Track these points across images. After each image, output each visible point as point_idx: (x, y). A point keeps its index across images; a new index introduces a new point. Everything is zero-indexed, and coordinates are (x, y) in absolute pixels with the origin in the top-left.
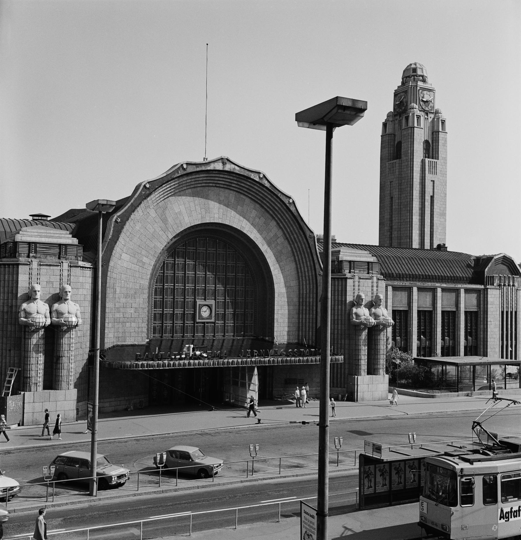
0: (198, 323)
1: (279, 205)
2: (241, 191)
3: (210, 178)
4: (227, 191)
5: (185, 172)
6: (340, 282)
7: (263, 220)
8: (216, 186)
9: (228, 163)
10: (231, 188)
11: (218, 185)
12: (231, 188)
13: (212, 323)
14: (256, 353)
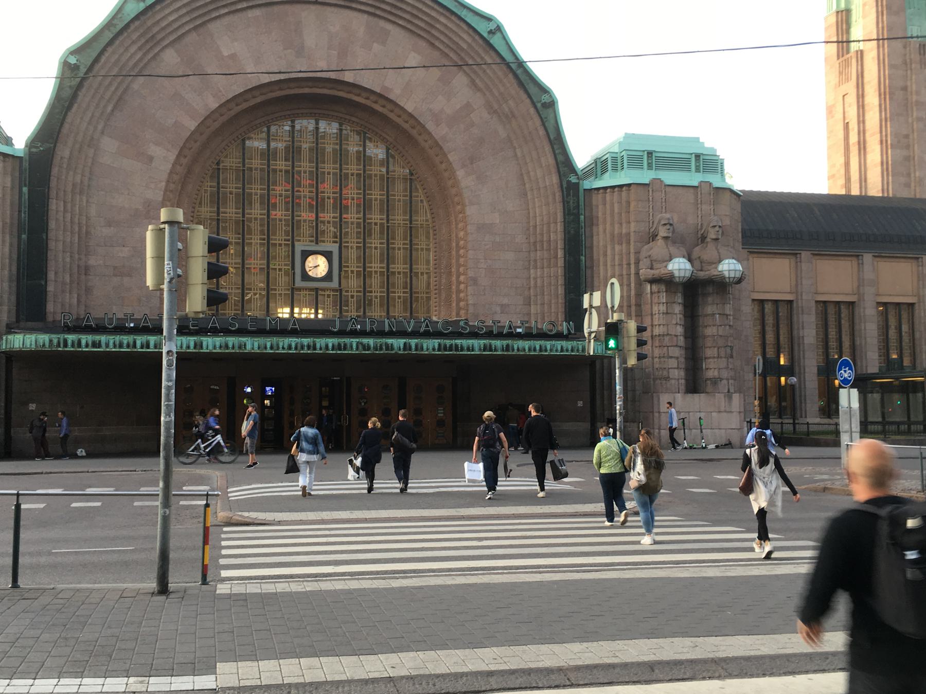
0: (299, 289)
1: (465, 36)
2: (378, 12)
7: (436, 72)
13: (334, 290)
14: (300, 313)
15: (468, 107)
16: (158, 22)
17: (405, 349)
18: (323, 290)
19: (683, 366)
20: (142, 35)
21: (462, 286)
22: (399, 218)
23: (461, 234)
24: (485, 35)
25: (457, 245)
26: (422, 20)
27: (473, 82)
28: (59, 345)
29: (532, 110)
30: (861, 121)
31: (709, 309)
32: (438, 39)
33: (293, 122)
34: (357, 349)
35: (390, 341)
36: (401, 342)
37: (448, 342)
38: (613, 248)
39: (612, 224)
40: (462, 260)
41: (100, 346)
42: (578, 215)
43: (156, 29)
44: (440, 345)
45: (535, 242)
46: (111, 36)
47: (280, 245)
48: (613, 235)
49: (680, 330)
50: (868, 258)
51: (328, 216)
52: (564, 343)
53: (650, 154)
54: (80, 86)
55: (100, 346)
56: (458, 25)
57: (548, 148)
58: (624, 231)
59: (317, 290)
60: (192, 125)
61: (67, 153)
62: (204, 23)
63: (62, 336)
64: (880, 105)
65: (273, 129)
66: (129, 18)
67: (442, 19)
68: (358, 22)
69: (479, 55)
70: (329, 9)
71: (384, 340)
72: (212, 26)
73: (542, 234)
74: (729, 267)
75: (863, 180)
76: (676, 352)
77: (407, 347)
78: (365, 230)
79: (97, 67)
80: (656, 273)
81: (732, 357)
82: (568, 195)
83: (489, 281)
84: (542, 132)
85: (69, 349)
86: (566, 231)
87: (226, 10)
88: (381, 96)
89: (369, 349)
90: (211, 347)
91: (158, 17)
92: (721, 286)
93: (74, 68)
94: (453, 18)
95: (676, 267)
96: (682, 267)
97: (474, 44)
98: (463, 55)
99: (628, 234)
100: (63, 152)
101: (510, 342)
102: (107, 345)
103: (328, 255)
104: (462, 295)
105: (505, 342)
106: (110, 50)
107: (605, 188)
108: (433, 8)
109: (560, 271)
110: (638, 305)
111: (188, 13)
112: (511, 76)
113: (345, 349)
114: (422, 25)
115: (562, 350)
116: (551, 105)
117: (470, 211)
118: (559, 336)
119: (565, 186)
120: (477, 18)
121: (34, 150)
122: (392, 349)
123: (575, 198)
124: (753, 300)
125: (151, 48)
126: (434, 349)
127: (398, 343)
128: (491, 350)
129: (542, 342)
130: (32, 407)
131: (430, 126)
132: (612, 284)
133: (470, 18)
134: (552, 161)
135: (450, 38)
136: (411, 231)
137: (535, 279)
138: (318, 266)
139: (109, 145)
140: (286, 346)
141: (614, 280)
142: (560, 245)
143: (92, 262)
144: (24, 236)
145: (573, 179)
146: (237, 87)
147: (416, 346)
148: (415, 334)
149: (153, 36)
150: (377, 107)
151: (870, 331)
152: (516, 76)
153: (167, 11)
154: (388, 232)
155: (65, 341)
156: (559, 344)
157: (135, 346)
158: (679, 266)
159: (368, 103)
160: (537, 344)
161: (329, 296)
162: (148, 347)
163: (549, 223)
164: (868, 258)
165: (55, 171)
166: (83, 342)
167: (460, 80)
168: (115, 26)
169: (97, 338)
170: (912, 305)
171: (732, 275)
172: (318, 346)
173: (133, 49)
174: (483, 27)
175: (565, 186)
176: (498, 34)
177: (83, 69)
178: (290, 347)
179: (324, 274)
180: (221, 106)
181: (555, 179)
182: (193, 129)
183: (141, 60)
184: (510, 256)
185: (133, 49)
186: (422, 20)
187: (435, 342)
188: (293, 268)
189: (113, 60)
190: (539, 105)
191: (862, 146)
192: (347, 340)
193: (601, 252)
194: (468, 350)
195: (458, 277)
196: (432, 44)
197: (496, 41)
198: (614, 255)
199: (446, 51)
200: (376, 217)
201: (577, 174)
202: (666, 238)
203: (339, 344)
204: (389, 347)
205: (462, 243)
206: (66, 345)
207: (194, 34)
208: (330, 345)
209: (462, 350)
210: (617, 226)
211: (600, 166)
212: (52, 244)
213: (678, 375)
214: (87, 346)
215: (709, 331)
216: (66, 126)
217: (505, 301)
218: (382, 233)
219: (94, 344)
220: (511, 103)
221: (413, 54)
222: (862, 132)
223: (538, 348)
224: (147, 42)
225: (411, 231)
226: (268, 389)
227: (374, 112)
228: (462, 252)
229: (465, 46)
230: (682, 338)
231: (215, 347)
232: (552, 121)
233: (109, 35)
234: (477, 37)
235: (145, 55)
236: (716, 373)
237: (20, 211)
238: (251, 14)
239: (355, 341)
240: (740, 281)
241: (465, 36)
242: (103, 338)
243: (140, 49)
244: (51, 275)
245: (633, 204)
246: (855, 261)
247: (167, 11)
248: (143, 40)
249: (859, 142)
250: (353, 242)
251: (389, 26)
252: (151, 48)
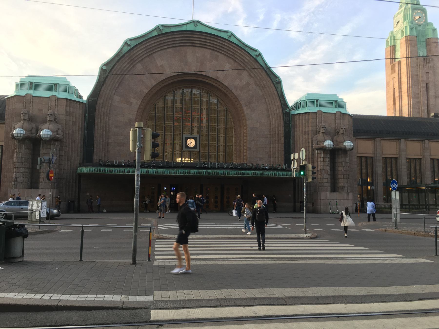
0: (185, 151)
1: (247, 57)
2: (215, 49)
3: (185, 38)
4: (203, 49)
5: (160, 33)
6: (301, 117)
8: (192, 46)
9: (199, 24)
10: (206, 47)
11: (194, 45)
12: (206, 47)
13: (197, 152)
14: (185, 160)
16: (135, 54)
17: (223, 174)
18: (194, 152)
19: (330, 182)
20: (129, 58)
21: (245, 151)
22: (222, 125)
23: (245, 131)
24: (255, 57)
25: (243, 135)
26: (231, 51)
27: (250, 74)
28: (98, 171)
29: (272, 85)
30: (400, 88)
31: (340, 160)
32: (237, 58)
33: (183, 90)
34: (206, 174)
35: (218, 171)
36: (222, 171)
37: (240, 172)
38: (303, 137)
39: (302, 127)
40: (245, 141)
41: (112, 172)
42: (289, 124)
43: (134, 57)
44: (236, 173)
45: (273, 134)
46: (118, 59)
47: (178, 135)
48: (302, 132)
49: (328, 168)
50: (403, 141)
51: (196, 124)
52: (284, 172)
53: (317, 101)
54: (107, 77)
55: (112, 172)
56: (244, 53)
57: (278, 99)
58: (307, 130)
59: (191, 152)
60: (146, 91)
61: (102, 101)
62: (151, 54)
63: (99, 168)
64: (407, 82)
65: (176, 92)
66: (125, 52)
67: (239, 51)
68: (208, 53)
69: (252, 64)
70: (197, 48)
71: (215, 171)
72: (154, 55)
73: (275, 131)
74: (348, 144)
75: (401, 110)
76: (327, 176)
77: (224, 173)
78: (209, 130)
79: (113, 70)
80: (319, 146)
81: (349, 178)
82: (286, 116)
83: (256, 149)
84: (276, 93)
85: (101, 173)
86: (285, 130)
87: (159, 49)
88: (215, 80)
89: (210, 174)
90: (152, 173)
91: (135, 52)
92: (345, 151)
93: (105, 70)
94: (243, 51)
95: (327, 144)
96: (329, 144)
97: (250, 60)
98: (246, 64)
99: (309, 131)
100: (100, 101)
101: (263, 172)
102: (115, 172)
103: (195, 139)
104: (245, 154)
105: (261, 172)
106: (118, 64)
107: (300, 114)
108: (235, 47)
109: (282, 145)
110: (312, 158)
111: (146, 50)
112: (264, 72)
113: (201, 174)
114: (231, 53)
115: (283, 175)
116: (279, 83)
117: (249, 122)
118: (282, 170)
119: (284, 113)
120: (251, 50)
121: (90, 100)
122: (219, 174)
123: (288, 118)
124: (357, 157)
125: (132, 63)
126: (234, 174)
127: (221, 172)
128: (256, 175)
129: (275, 172)
130: (88, 194)
131: (234, 91)
132: (303, 150)
133: (249, 51)
134: (279, 103)
135: (241, 58)
136: (226, 130)
137: (273, 148)
138: (191, 143)
139: (117, 98)
140: (179, 172)
141: (303, 149)
142: (282, 135)
143: (110, 141)
144: (86, 132)
145: (288, 110)
146: (163, 77)
147: (228, 173)
148: (227, 168)
149: (133, 59)
150: (214, 84)
151: (404, 168)
152: (266, 72)
153: (138, 50)
154: (217, 130)
155: (100, 170)
156: (282, 173)
157: (125, 172)
158: (328, 143)
159: (211, 82)
160: (273, 173)
161: (195, 154)
162: (129, 172)
163: (278, 127)
164: (403, 141)
165: (97, 108)
166: (106, 170)
167: (245, 74)
168: (119, 55)
169: (111, 169)
170: (421, 159)
171: (349, 147)
172: (191, 173)
173: (126, 64)
174: (254, 54)
175: (284, 113)
176: (260, 57)
177: (108, 71)
178: (181, 173)
179: (194, 146)
180: (157, 84)
181: (281, 110)
182: (147, 92)
183: (129, 67)
185: (126, 64)
186: (231, 51)
187: (235, 172)
188: (182, 144)
189: (118, 68)
190: (275, 83)
191: (400, 98)
192: (202, 171)
193: (298, 138)
194: (247, 174)
195: (243, 147)
196: (235, 61)
197: (259, 59)
198: (303, 139)
199: (240, 63)
200: (213, 125)
201: (289, 109)
202: (323, 133)
203: (199, 172)
204: (218, 173)
205: (245, 134)
206: (100, 171)
207: (148, 58)
208: (196, 173)
209: (245, 174)
210: (304, 128)
211: (298, 105)
212: (96, 135)
213: (328, 185)
214: (108, 172)
215: (340, 168)
216: (102, 92)
217: (261, 156)
218: (215, 130)
219: (110, 171)
220: (264, 82)
221: (228, 64)
222: (400, 92)
223: (274, 174)
224: (131, 61)
225: (226, 130)
226: (172, 188)
227: (213, 85)
228: (245, 138)
229: (247, 61)
230: (329, 171)
231: (153, 173)
232: (280, 89)
233: (117, 59)
234: (251, 58)
235: (130, 65)
236: (343, 185)
237: (85, 122)
238: (168, 50)
239: (205, 171)
240: (352, 149)
241: (247, 57)
242: (113, 169)
243: (128, 63)
244: (95, 146)
245: (310, 120)
246: (398, 142)
247: (138, 50)
248: (129, 60)
249: (399, 96)
250: (204, 134)
251: (219, 54)
252: (132, 63)
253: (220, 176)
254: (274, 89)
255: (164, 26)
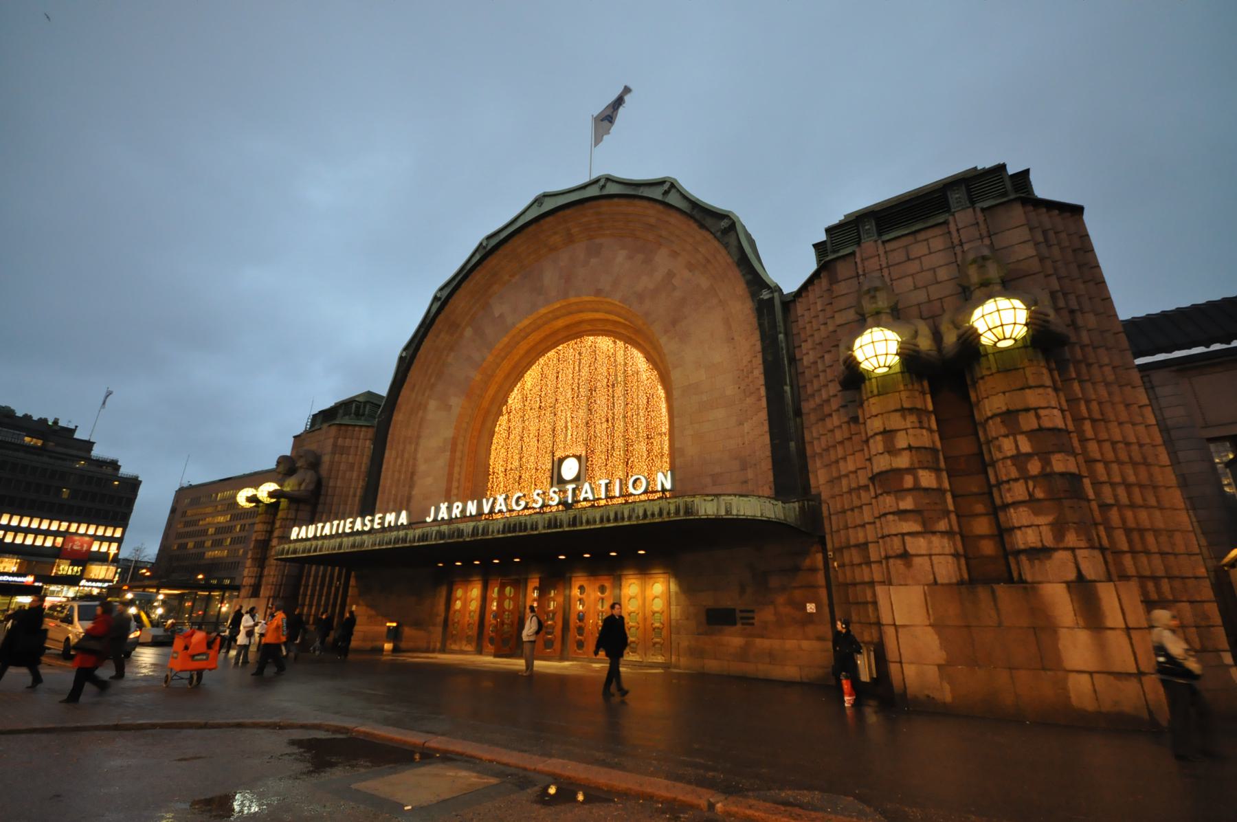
15: (670, 275)
24: (660, 198)
139: (432, 404)
174: (657, 193)
176: (673, 191)
184: (720, 414)
204: (460, 533)
253: (465, 542)
254: (724, 252)
255: (489, 238)
